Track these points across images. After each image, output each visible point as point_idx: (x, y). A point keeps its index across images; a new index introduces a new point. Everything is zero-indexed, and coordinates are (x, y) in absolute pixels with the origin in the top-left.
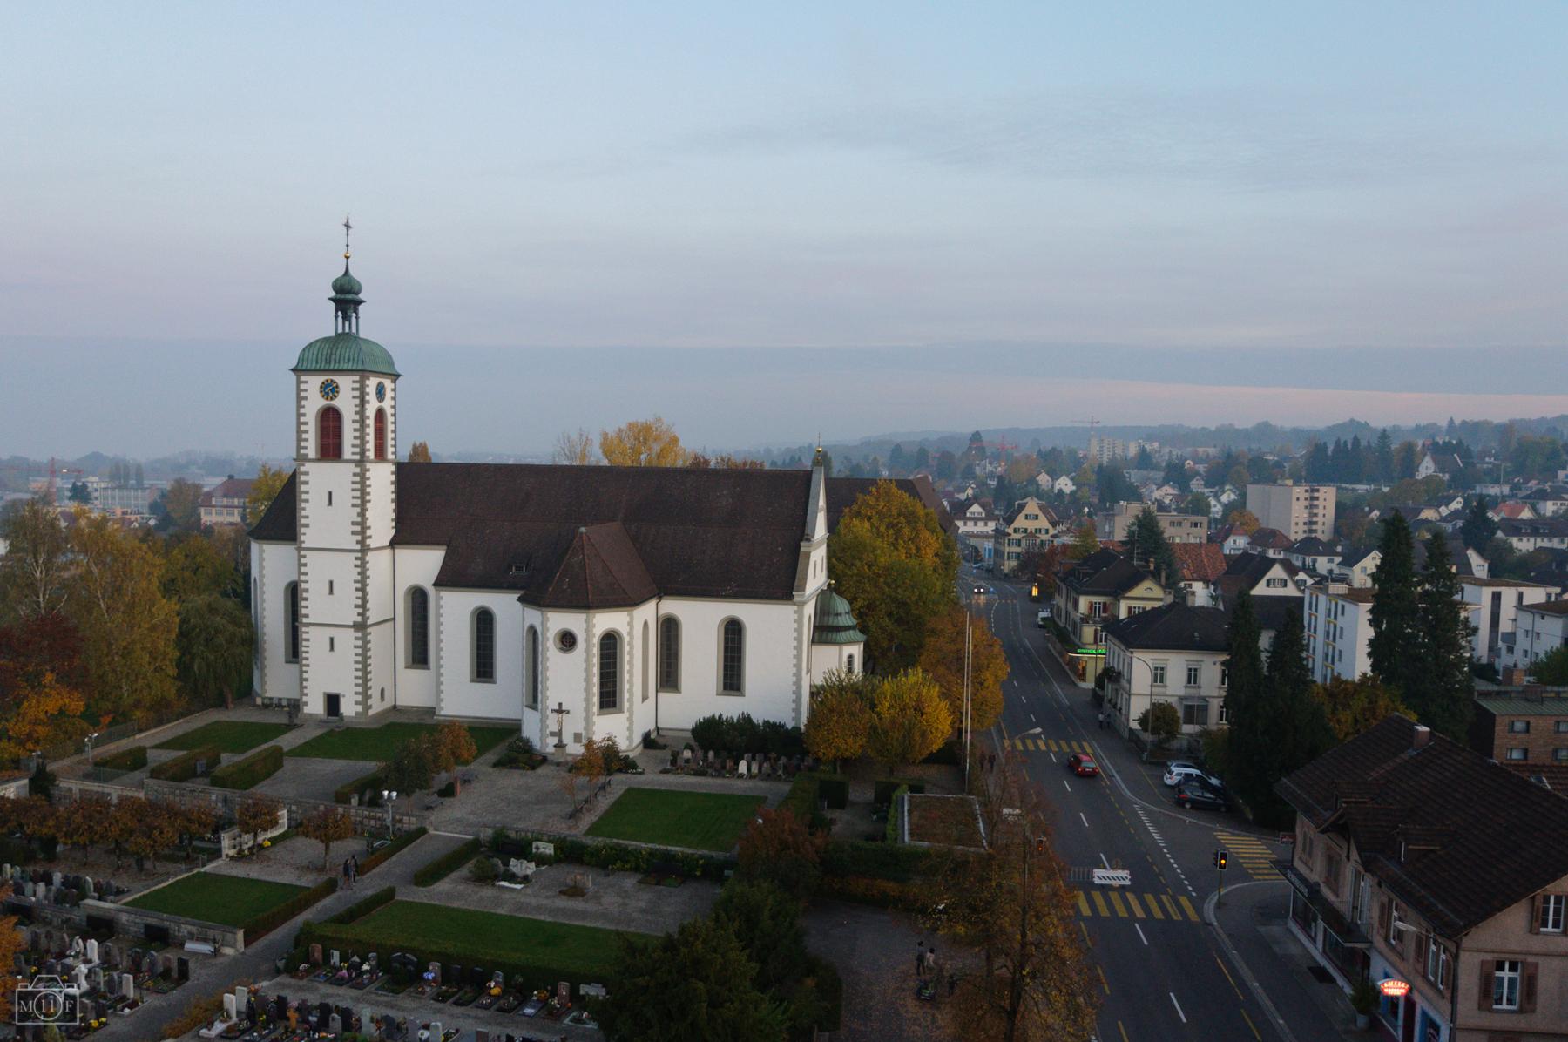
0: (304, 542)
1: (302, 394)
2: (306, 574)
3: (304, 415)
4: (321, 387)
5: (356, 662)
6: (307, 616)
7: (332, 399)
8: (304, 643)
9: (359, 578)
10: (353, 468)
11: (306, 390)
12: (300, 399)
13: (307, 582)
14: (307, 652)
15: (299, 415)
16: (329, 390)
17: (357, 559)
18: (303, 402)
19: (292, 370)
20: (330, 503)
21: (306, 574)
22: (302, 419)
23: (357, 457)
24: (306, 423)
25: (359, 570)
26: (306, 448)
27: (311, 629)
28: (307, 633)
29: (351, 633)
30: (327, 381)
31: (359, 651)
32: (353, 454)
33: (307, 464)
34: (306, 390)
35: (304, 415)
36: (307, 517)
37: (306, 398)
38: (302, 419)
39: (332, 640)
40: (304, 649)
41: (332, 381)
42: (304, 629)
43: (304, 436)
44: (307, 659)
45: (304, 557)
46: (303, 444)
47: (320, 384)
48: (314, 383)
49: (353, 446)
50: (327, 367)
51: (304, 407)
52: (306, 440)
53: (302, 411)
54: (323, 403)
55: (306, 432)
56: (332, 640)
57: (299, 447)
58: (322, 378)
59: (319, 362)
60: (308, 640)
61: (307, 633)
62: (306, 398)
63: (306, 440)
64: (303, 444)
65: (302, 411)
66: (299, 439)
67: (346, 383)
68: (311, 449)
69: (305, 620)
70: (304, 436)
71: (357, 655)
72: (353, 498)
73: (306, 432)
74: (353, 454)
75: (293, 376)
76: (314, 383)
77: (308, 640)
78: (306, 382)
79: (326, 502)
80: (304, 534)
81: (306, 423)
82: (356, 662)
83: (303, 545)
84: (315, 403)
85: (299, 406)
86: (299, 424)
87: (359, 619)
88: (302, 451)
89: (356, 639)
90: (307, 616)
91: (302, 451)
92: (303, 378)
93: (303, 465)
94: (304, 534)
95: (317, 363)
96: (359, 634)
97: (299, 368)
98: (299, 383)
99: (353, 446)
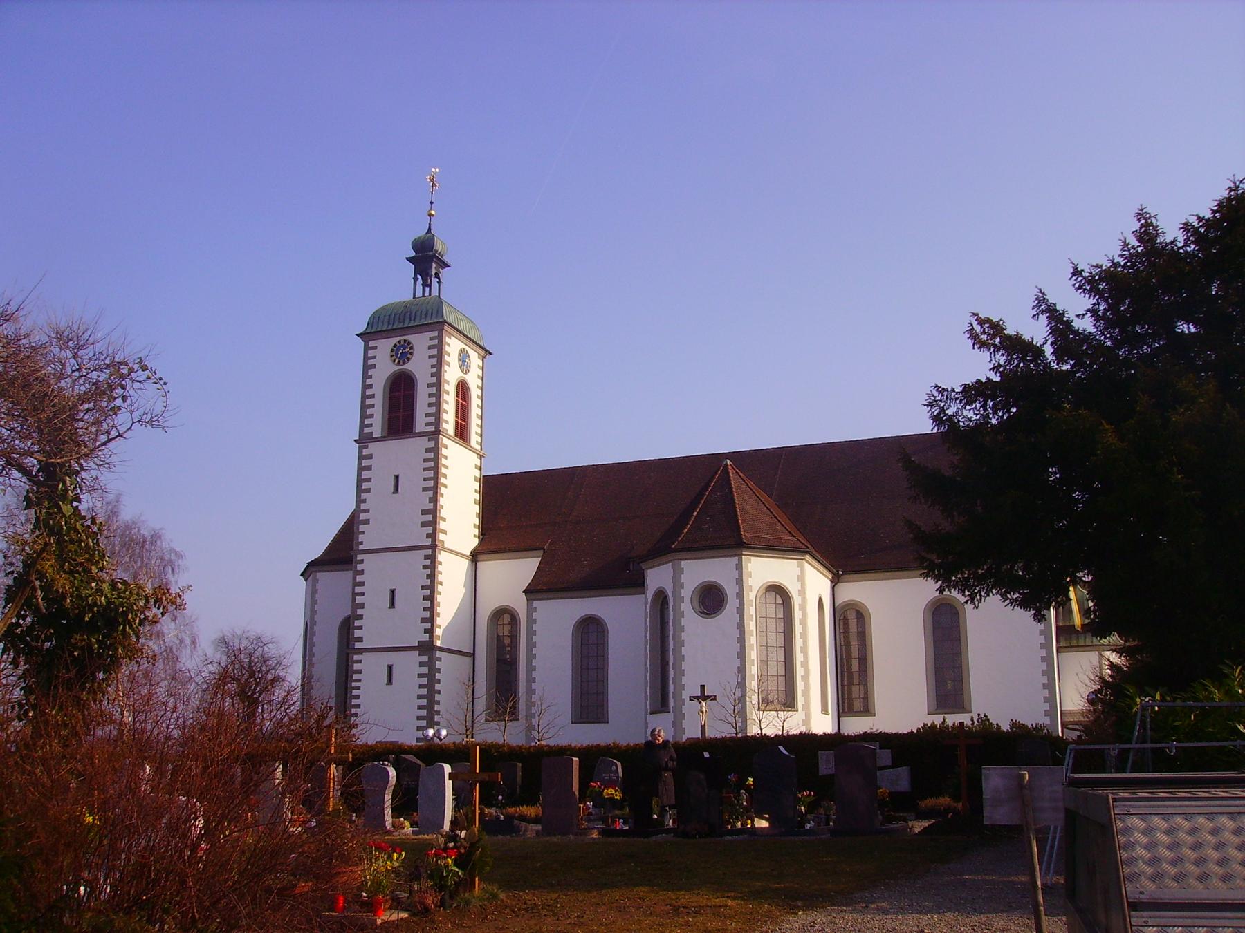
0: (362, 543)
1: (370, 362)
2: (362, 584)
3: (370, 386)
4: (392, 351)
5: (420, 697)
6: (360, 639)
7: (404, 363)
8: (355, 676)
9: (428, 582)
10: (425, 443)
11: (374, 357)
12: (367, 368)
13: (363, 594)
14: (358, 688)
15: (365, 387)
16: (402, 353)
17: (426, 557)
18: (370, 372)
19: (358, 335)
20: (396, 490)
21: (362, 584)
22: (368, 392)
23: (432, 428)
24: (372, 396)
25: (428, 571)
26: (371, 425)
27: (364, 657)
28: (360, 662)
29: (415, 657)
30: (399, 342)
31: (425, 681)
32: (427, 425)
34: (374, 357)
35: (370, 386)
36: (367, 511)
37: (374, 366)
38: (368, 392)
39: (390, 668)
40: (354, 684)
41: (405, 341)
42: (356, 657)
43: (369, 412)
44: (357, 697)
46: (367, 421)
47: (391, 346)
48: (384, 347)
49: (427, 415)
50: (401, 326)
51: (371, 377)
52: (372, 416)
53: (368, 382)
55: (372, 406)
56: (390, 668)
57: (363, 425)
58: (395, 340)
59: (391, 322)
60: (360, 672)
61: (360, 662)
62: (374, 366)
63: (372, 416)
64: (367, 421)
65: (368, 382)
66: (364, 416)
67: (420, 342)
69: (358, 645)
70: (369, 412)
71: (421, 686)
72: (425, 479)
73: (372, 406)
74: (427, 425)
75: (360, 343)
76: (384, 347)
77: (360, 672)
78: (375, 348)
79: (392, 489)
80: (363, 533)
81: (372, 396)
82: (420, 697)
84: (385, 368)
85: (366, 376)
86: (364, 397)
87: (426, 637)
88: (366, 430)
89: (422, 664)
90: (360, 639)
91: (366, 430)
92: (371, 344)
93: (367, 447)
94: (363, 533)
95: (389, 324)
96: (425, 658)
97: (368, 331)
98: (367, 349)
99: (427, 415)
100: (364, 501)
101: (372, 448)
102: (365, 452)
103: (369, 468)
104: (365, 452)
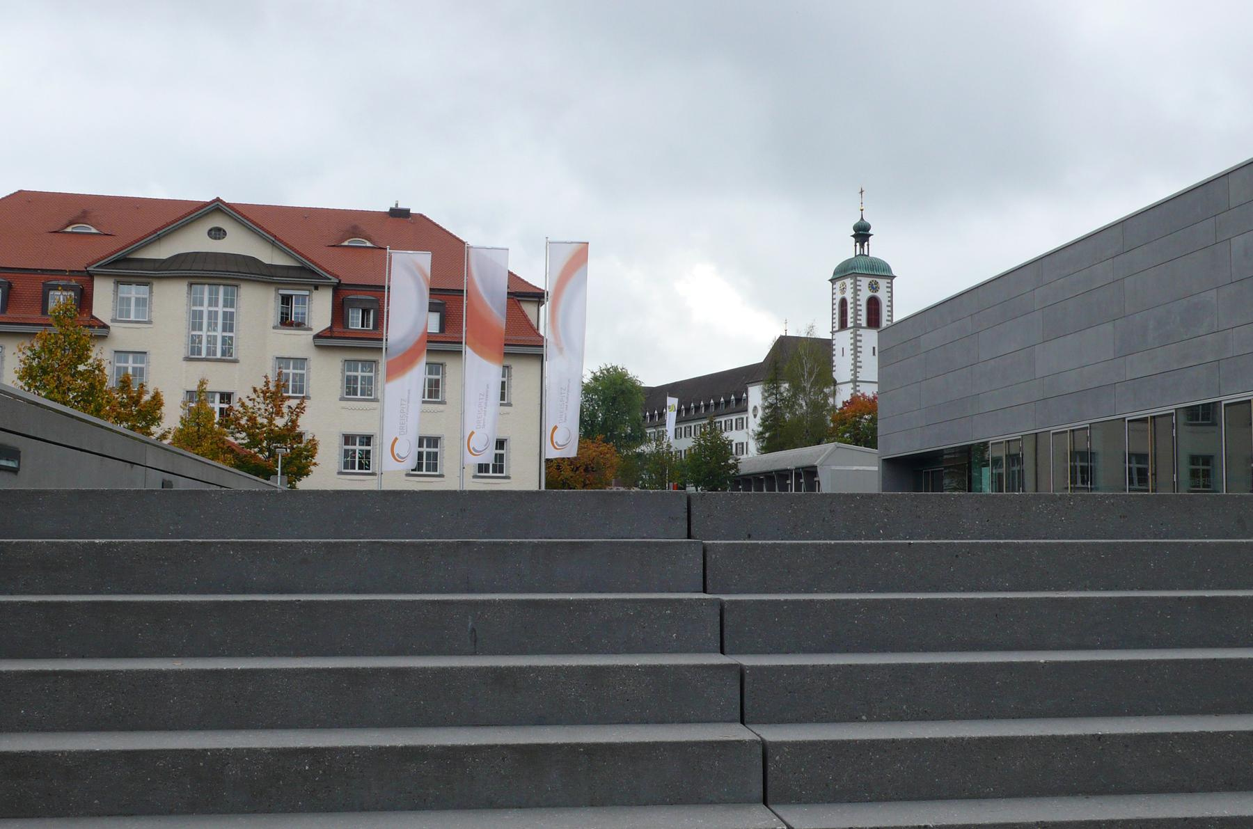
3: (859, 300)
26: (860, 320)
33: (861, 330)
35: (859, 300)
36: (860, 362)
37: (860, 290)
43: (859, 313)
45: (859, 386)
54: (870, 294)
62: (860, 290)
63: (861, 315)
64: (858, 317)
67: (882, 283)
68: (864, 322)
70: (859, 313)
78: (860, 281)
83: (858, 379)
88: (858, 322)
100: (859, 357)
101: (861, 332)
102: (858, 333)
103: (860, 341)
104: (858, 333)
